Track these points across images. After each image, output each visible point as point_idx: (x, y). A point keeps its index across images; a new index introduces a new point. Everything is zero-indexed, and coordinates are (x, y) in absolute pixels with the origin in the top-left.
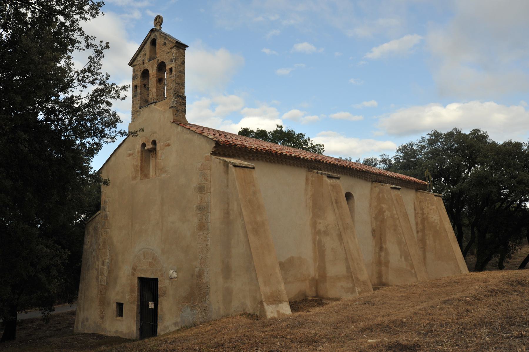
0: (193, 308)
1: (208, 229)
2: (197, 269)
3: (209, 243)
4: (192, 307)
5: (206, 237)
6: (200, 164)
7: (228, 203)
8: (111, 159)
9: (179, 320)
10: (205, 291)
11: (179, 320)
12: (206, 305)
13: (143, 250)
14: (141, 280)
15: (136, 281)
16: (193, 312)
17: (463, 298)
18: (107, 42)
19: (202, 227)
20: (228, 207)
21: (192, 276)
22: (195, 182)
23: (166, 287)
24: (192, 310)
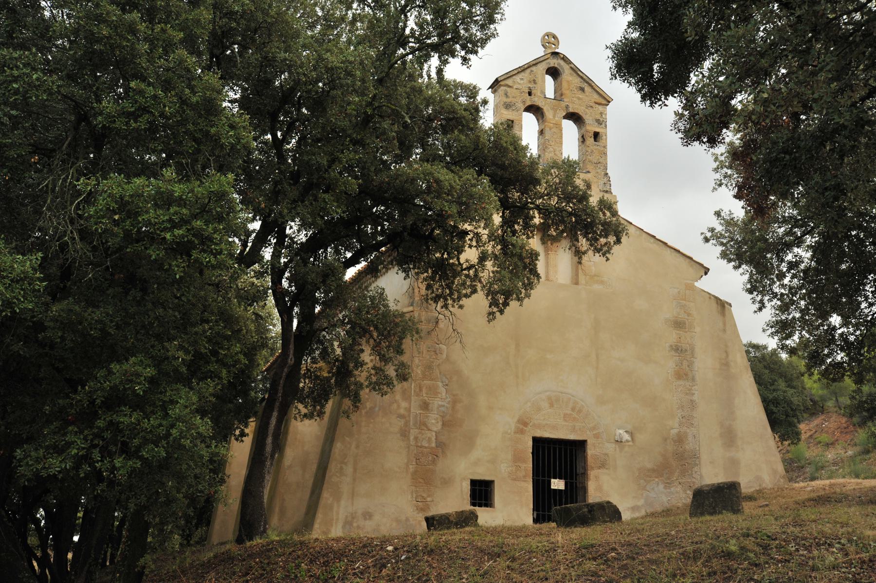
0: (668, 485)
1: (693, 379)
2: (674, 432)
3: (695, 398)
4: (667, 483)
5: (691, 390)
6: (676, 291)
7: (726, 352)
8: (668, 249)
9: (641, 502)
10: (690, 462)
11: (641, 502)
12: (694, 480)
13: (548, 393)
14: (538, 443)
15: (528, 445)
16: (668, 490)
17: (414, 561)
18: (548, 35)
19: (684, 374)
20: (727, 356)
21: (666, 440)
22: (668, 311)
23: (606, 454)
24: (665, 487)
